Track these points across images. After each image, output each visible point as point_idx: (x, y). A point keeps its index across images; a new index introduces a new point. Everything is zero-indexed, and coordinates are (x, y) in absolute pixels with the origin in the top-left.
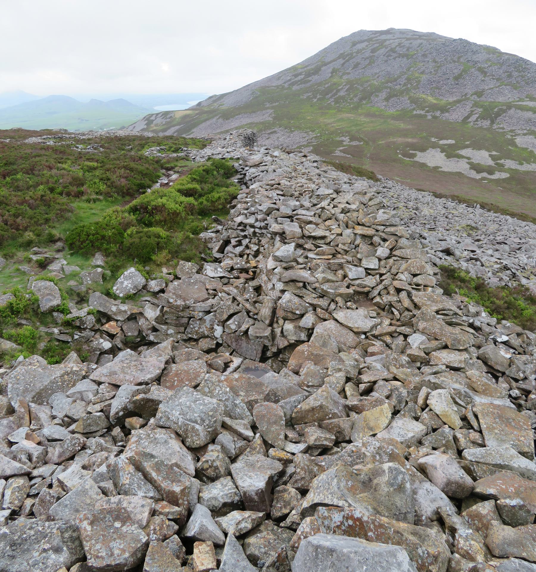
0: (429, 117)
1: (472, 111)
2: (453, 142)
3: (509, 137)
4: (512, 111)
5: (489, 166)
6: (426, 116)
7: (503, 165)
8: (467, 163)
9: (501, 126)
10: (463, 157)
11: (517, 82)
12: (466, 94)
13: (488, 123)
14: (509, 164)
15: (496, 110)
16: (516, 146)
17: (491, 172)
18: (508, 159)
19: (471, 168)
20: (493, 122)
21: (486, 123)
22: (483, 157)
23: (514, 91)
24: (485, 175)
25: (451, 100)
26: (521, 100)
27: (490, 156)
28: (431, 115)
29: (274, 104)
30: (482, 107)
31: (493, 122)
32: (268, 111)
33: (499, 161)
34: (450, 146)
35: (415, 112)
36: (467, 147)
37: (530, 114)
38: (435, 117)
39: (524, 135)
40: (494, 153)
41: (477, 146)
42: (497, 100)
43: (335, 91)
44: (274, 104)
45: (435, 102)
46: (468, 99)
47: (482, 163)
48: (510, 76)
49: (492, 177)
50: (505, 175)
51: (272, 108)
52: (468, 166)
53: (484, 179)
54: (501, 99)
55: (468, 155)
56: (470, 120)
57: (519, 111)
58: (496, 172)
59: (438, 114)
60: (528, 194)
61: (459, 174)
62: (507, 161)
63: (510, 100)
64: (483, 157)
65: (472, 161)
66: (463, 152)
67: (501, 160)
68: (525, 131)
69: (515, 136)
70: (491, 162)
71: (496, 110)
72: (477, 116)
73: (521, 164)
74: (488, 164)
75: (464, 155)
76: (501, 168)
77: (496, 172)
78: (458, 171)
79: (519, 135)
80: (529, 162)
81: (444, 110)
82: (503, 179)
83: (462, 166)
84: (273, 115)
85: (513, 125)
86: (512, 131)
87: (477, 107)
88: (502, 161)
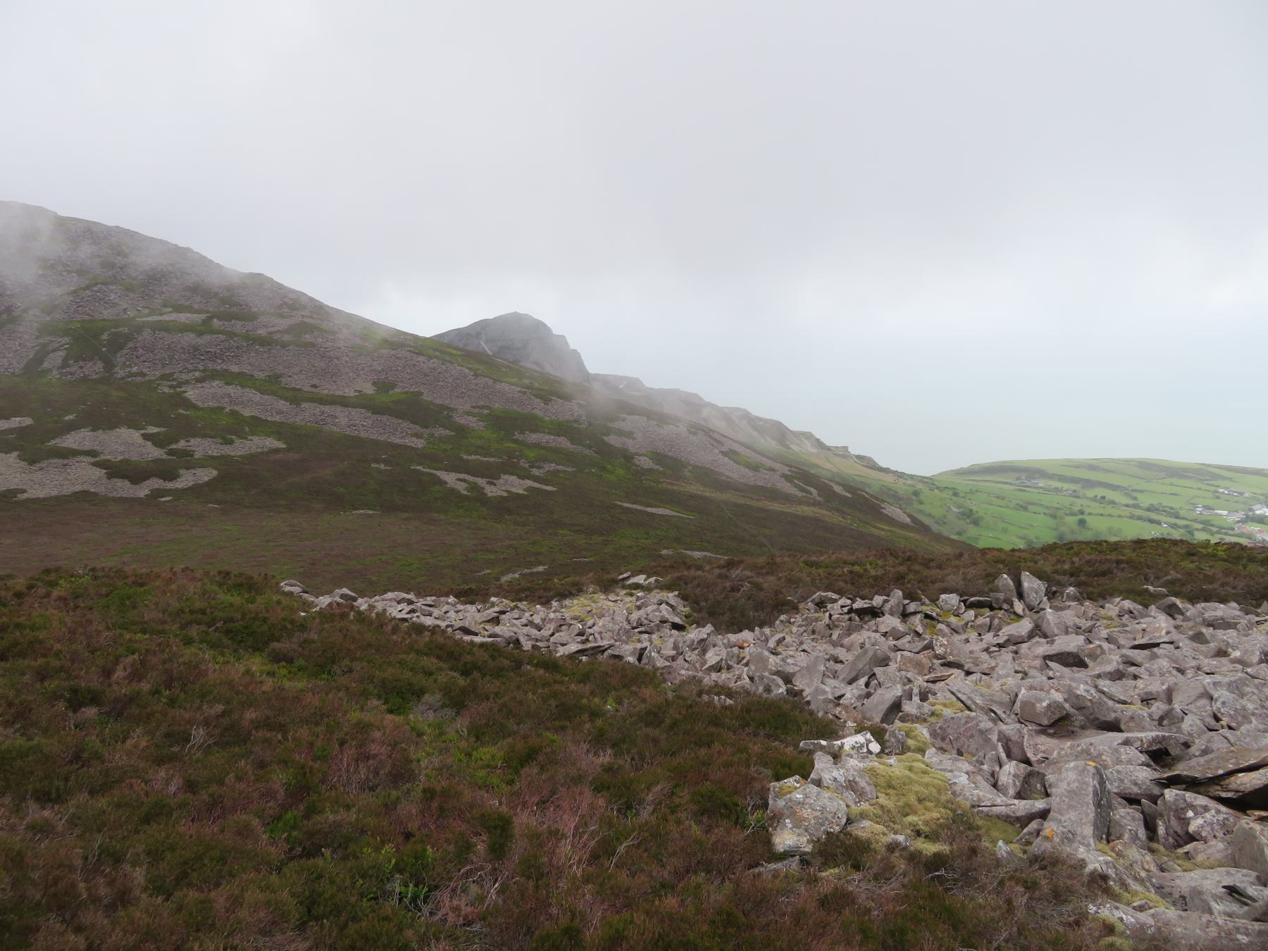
1: (44, 346)
2: (28, 421)
3: (167, 390)
4: (146, 334)
5: (156, 461)
7: (188, 454)
8: (94, 464)
9: (135, 369)
10: (74, 453)
13: (99, 366)
14: (201, 447)
15: (105, 337)
16: (195, 407)
17: (170, 475)
18: (194, 436)
19: (110, 476)
20: (109, 365)
21: (95, 369)
22: (127, 442)
23: (131, 295)
24: (156, 483)
27: (146, 437)
33: (174, 446)
34: (22, 431)
36: (71, 427)
37: (190, 338)
39: (198, 380)
40: (152, 430)
41: (102, 419)
47: (135, 457)
49: (179, 484)
50: (206, 475)
52: (101, 473)
53: (157, 493)
55: (87, 445)
56: (46, 365)
57: (163, 334)
58: (182, 472)
60: (283, 502)
61: (84, 496)
62: (194, 441)
64: (127, 442)
65: (102, 457)
66: (70, 441)
67: (177, 442)
68: (197, 374)
69: (180, 385)
70: (155, 453)
71: (105, 337)
73: (231, 442)
74: (150, 457)
75: (75, 446)
76: (187, 460)
77: (182, 472)
78: (78, 488)
79: (187, 382)
80: (242, 436)
82: (207, 484)
83: (84, 476)
85: (164, 365)
86: (164, 377)
88: (182, 444)
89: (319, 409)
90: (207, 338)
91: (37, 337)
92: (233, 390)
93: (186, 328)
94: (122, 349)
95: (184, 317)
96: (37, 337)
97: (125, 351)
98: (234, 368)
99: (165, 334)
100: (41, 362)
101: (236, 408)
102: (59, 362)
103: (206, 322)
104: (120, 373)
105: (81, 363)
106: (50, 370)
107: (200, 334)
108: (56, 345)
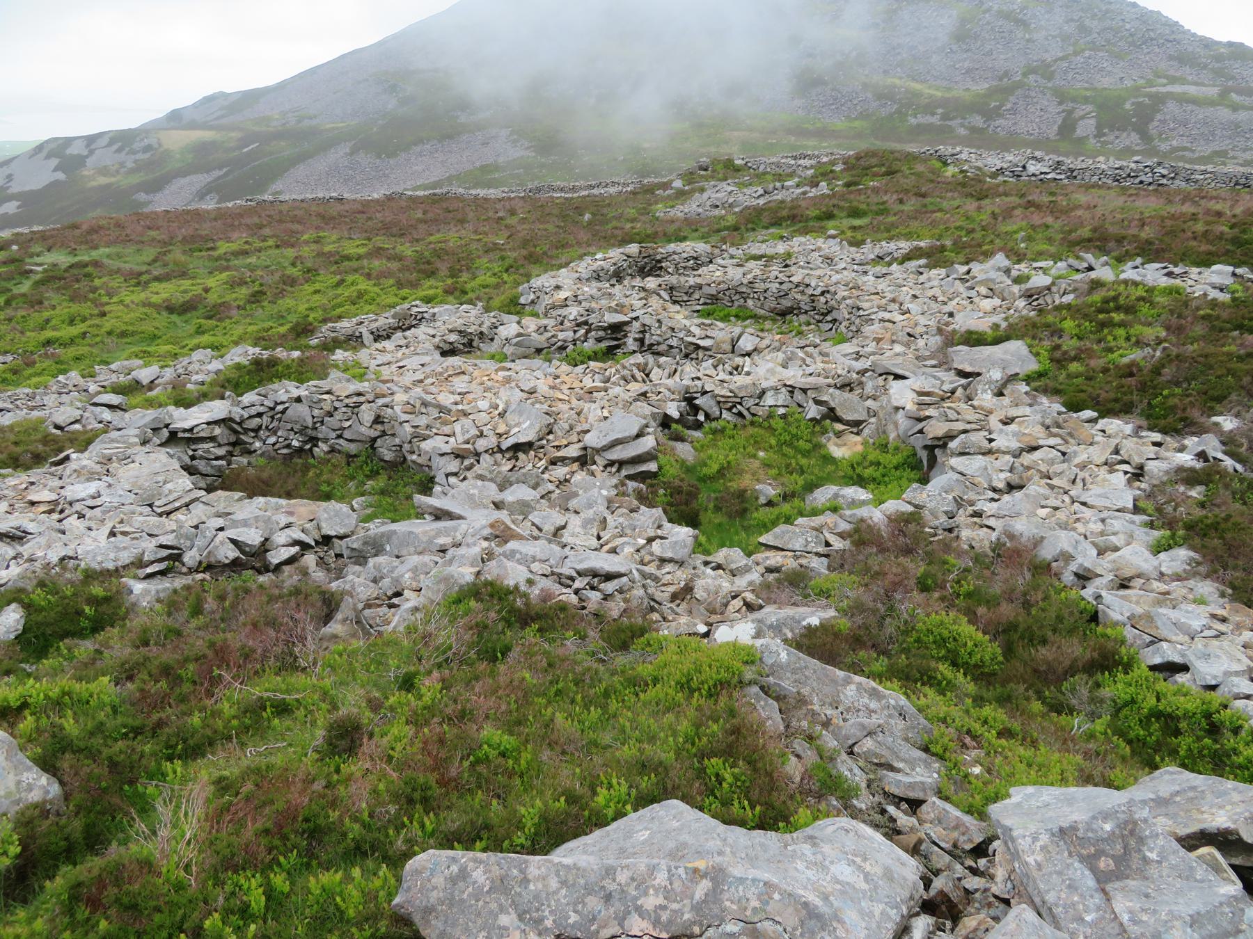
0: (962, 132)
1: (1070, 112)
4: (1172, 106)
6: (951, 130)
9: (1174, 143)
11: (1108, 41)
12: (1006, 74)
13: (1135, 137)
15: (1128, 106)
25: (982, 87)
26: (1150, 84)
28: (962, 125)
30: (1086, 100)
31: (1145, 136)
35: (913, 121)
37: (1224, 113)
38: (974, 130)
42: (1099, 86)
45: (939, 94)
46: (1020, 85)
48: (1083, 29)
54: (1105, 82)
56: (1080, 132)
59: (978, 121)
63: (1129, 83)
72: (1093, 121)
84: (527, 144)
87: (1074, 100)
91: (1060, 103)
93: (1212, 103)
94: (1152, 120)
95: (1192, 90)
96: (1060, 103)
99: (1194, 107)
100: (1074, 129)
103: (1224, 93)
104: (1164, 147)
105: (1117, 133)
107: (1235, 108)
108: (1082, 113)
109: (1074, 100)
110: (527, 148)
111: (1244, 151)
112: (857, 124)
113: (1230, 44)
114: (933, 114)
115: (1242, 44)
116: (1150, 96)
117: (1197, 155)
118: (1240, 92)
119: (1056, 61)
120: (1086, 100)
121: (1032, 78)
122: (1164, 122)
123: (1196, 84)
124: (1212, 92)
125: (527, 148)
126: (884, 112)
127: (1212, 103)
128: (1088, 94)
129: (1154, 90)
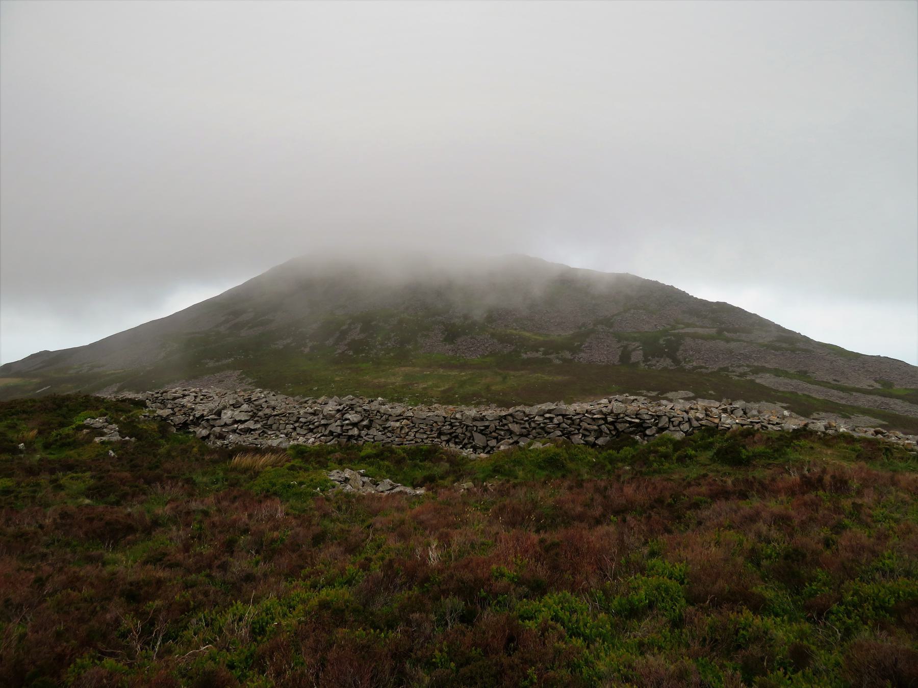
1: (625, 347)
4: (688, 341)
6: (550, 361)
9: (695, 364)
12: (583, 325)
15: (661, 342)
26: (674, 328)
28: (558, 358)
29: (225, 362)
30: (635, 339)
31: (676, 361)
32: (229, 373)
35: (524, 356)
37: (721, 344)
38: (565, 360)
43: (337, 334)
44: (225, 362)
45: (541, 339)
51: (228, 367)
56: (633, 359)
57: (700, 341)
59: (567, 355)
63: (660, 328)
72: (641, 352)
81: (574, 350)
84: (250, 380)
87: (627, 339)
89: (870, 397)
90: (733, 345)
92: (782, 380)
93: (712, 338)
95: (700, 331)
96: (619, 342)
97: (680, 352)
98: (767, 365)
101: (806, 393)
102: (641, 358)
103: (720, 332)
104: (688, 366)
105: (657, 359)
106: (638, 362)
107: (728, 340)
109: (627, 339)
110: (250, 384)
111: (739, 367)
112: (488, 360)
113: (718, 303)
114: (537, 351)
115: (725, 303)
116: (674, 335)
117: (710, 371)
118: (728, 331)
119: (613, 316)
120: (635, 339)
121: (599, 327)
122: (686, 351)
123: (702, 327)
124: (713, 331)
125: (250, 384)
126: (505, 351)
127: (712, 338)
128: (636, 335)
129: (676, 331)
